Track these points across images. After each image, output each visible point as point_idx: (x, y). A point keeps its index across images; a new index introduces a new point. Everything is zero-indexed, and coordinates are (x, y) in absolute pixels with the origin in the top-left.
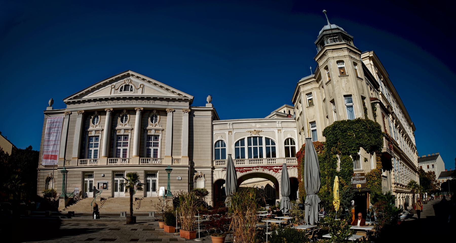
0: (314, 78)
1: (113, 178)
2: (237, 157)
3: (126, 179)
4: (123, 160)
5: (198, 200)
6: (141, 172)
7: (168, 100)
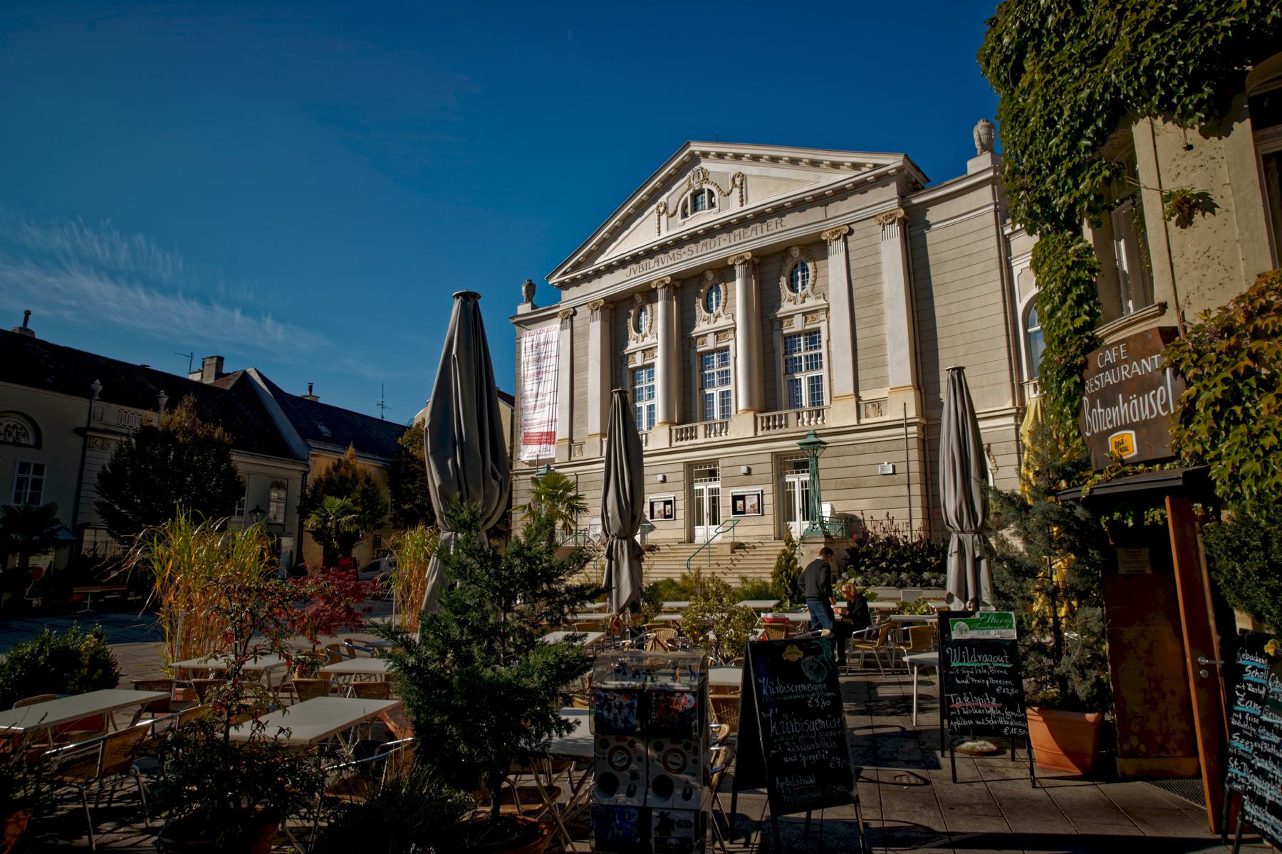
7: (821, 199)
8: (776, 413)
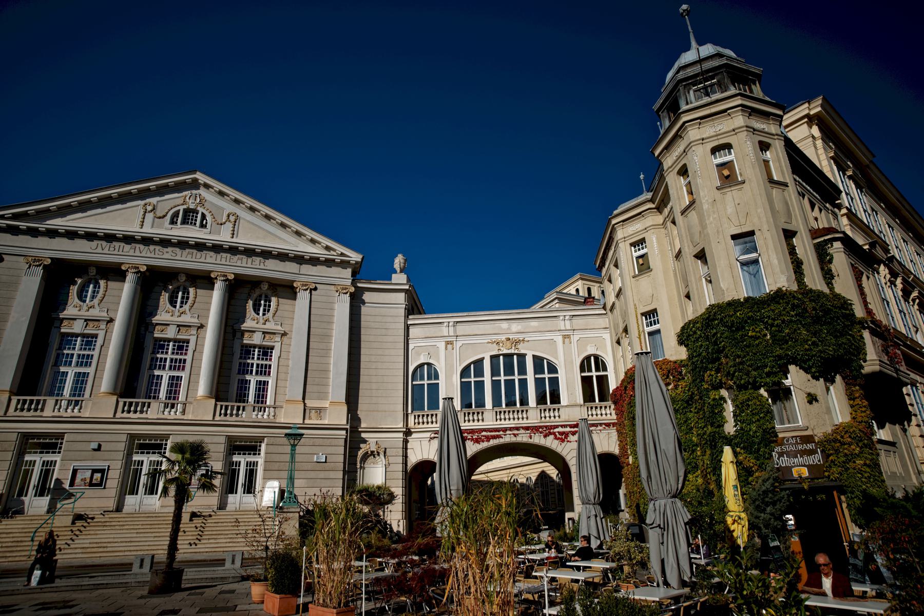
0: (652, 200)
1: (129, 455)
2: (466, 405)
3: (169, 460)
4: (166, 406)
5: (365, 515)
6: (216, 439)
7: (300, 259)
8: (35, 398)
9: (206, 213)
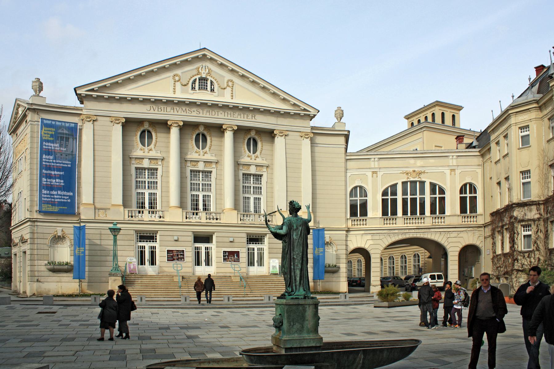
9: (213, 80)
